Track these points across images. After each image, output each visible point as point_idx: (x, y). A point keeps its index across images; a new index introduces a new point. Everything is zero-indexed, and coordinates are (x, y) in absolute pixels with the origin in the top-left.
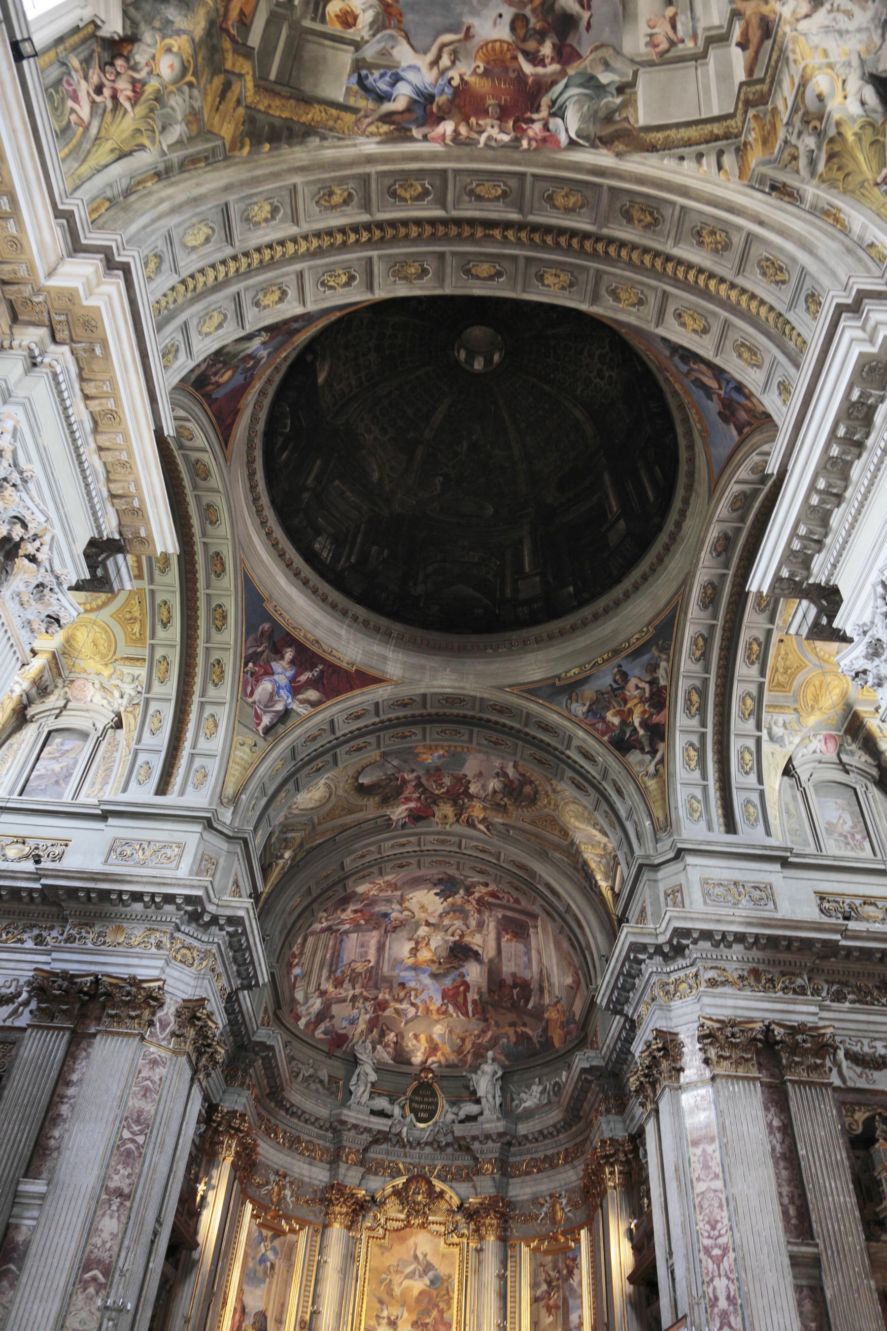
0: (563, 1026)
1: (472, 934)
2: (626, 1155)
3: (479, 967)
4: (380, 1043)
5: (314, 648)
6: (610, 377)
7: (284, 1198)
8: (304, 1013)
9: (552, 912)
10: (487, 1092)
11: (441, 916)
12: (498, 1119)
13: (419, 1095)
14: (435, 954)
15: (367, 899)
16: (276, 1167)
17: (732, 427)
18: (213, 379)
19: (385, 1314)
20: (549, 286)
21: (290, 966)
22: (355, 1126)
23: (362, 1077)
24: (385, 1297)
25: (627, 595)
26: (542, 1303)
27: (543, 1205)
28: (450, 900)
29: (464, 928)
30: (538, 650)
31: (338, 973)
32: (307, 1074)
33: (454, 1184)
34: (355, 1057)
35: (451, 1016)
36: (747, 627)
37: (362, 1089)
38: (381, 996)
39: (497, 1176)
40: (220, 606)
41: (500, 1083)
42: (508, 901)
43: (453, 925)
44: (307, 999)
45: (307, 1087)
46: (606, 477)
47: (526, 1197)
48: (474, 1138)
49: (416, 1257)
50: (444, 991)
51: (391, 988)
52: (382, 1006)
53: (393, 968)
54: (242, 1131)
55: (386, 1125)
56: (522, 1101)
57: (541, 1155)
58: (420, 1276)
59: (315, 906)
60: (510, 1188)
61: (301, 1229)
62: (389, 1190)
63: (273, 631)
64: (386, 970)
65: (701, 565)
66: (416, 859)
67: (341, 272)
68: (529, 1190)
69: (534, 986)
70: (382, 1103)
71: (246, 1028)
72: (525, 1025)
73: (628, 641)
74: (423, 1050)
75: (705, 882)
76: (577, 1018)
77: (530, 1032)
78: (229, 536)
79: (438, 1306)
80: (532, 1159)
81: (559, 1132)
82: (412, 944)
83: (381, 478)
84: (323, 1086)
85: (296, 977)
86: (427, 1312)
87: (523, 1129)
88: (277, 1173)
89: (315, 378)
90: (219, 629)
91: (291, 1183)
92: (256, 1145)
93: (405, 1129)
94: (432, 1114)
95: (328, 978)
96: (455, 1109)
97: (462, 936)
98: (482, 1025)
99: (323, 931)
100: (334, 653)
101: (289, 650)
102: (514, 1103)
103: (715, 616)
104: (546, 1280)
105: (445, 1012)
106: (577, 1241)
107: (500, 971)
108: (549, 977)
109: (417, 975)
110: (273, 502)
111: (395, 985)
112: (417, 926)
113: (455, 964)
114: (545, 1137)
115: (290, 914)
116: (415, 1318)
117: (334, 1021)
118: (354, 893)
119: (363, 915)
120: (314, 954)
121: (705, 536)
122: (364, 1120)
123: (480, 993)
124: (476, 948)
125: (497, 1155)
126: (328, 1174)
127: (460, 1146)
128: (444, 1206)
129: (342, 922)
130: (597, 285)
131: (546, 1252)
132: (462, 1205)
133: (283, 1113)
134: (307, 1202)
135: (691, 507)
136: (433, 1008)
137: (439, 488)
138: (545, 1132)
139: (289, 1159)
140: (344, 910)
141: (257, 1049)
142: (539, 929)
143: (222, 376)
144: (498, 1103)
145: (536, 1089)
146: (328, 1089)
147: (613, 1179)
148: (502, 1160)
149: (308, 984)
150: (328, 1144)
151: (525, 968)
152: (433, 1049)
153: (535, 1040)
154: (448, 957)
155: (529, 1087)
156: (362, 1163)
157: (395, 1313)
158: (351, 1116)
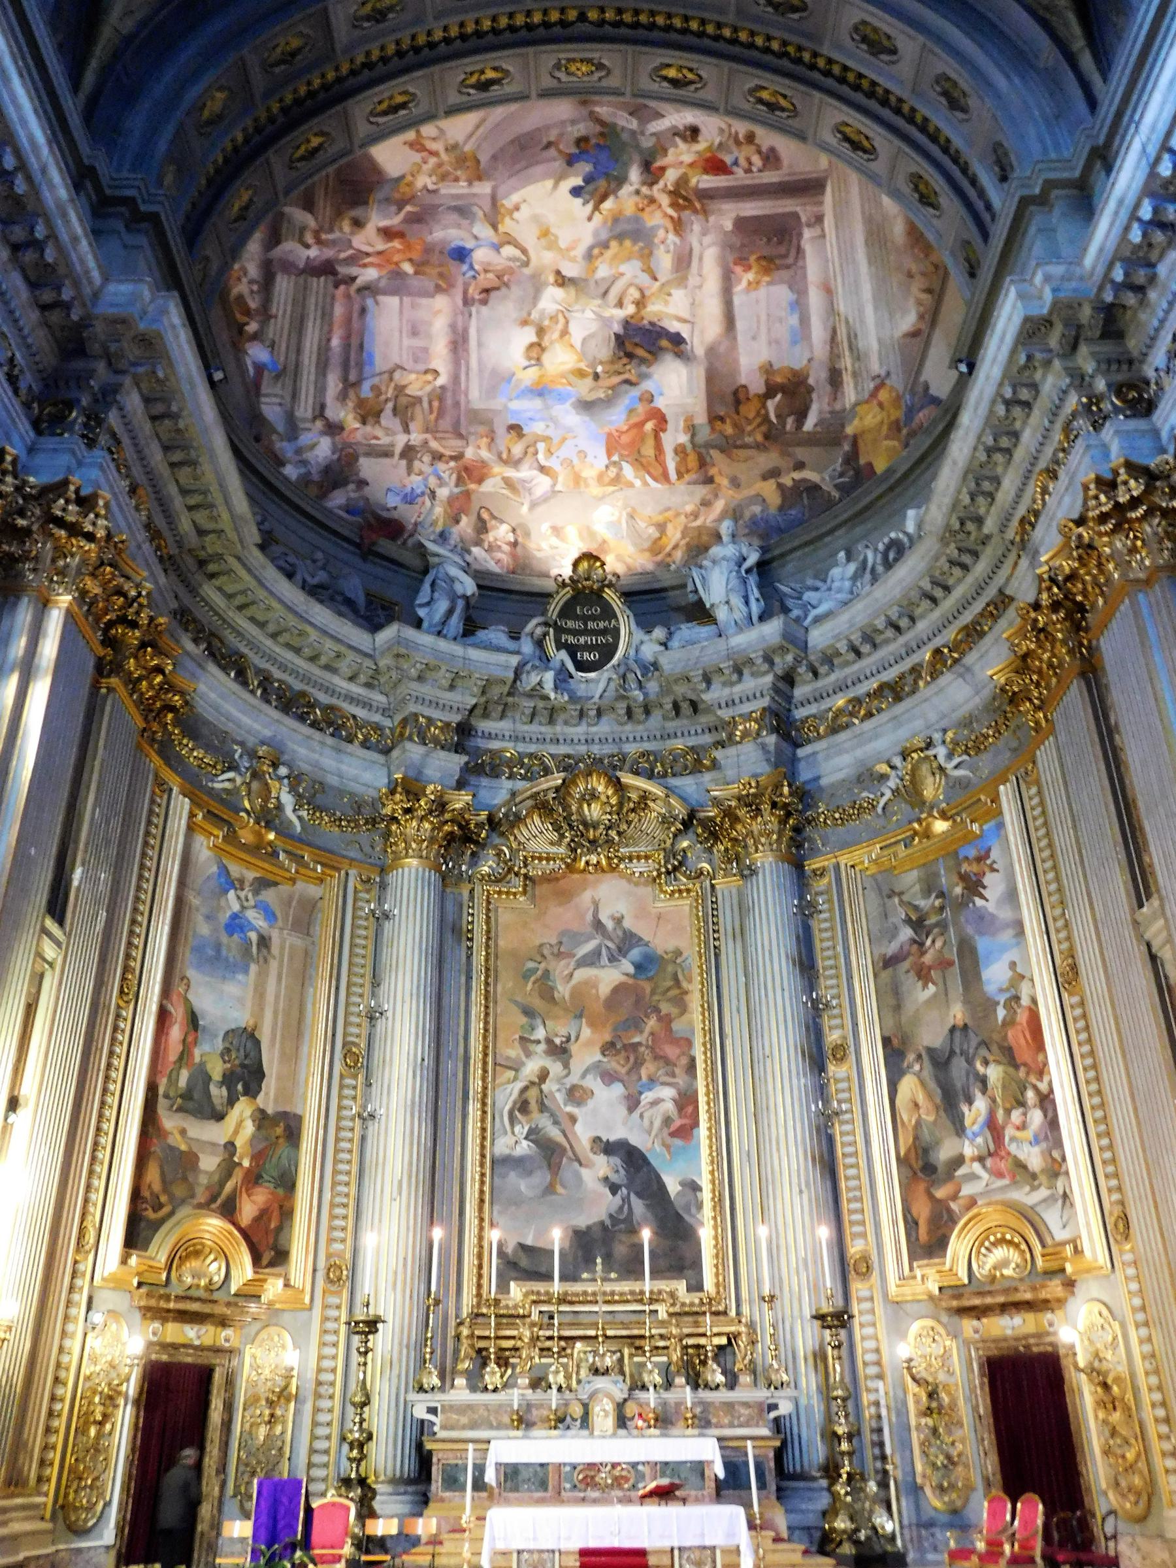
0: (896, 427)
4: (478, 543)
7: (279, 807)
11: (589, 256)
13: (576, 618)
14: (583, 355)
19: (540, 1033)
24: (537, 1003)
26: (906, 965)
27: (883, 777)
28: (608, 205)
29: (644, 280)
31: (366, 390)
33: (674, 782)
38: (469, 453)
41: (753, 580)
42: (748, 171)
43: (614, 279)
47: (840, 776)
49: (598, 925)
50: (609, 435)
56: (807, 607)
58: (612, 959)
60: (802, 766)
64: (475, 395)
69: (817, 377)
72: (800, 466)
79: (657, 1010)
82: (529, 335)
84: (356, 611)
85: (260, 368)
86: (636, 1024)
94: (608, 652)
95: (343, 397)
97: (640, 304)
98: (702, 491)
104: (908, 921)
107: (734, 371)
108: (852, 338)
109: (547, 407)
111: (501, 430)
113: (632, 373)
116: (608, 1037)
119: (409, 247)
120: (299, 325)
123: (692, 429)
124: (674, 326)
125: (765, 702)
127: (676, 707)
129: (357, 258)
132: (692, 815)
136: (589, 473)
140: (358, 224)
142: (829, 222)
144: (755, 609)
145: (842, 572)
149: (295, 395)
150: (377, 718)
151: (794, 343)
154: (615, 359)
157: (563, 1031)
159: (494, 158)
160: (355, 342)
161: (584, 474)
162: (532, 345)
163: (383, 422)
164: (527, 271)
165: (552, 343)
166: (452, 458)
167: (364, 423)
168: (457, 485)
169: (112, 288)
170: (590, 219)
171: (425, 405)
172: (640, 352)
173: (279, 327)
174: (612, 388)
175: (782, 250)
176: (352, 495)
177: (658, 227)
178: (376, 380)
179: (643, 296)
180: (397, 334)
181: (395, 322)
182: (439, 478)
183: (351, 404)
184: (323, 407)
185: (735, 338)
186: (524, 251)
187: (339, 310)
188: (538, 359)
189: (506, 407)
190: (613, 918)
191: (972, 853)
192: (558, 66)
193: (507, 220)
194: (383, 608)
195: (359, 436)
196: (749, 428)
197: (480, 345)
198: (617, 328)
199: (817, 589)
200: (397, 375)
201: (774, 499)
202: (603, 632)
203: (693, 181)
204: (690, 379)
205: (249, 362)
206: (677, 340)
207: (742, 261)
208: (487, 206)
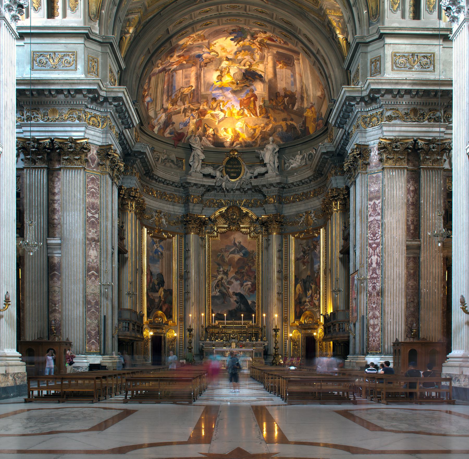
1: (257, 64)
2: (344, 196)
3: (262, 85)
4: (204, 135)
7: (162, 223)
8: (156, 123)
9: (309, 52)
10: (270, 161)
11: (236, 53)
12: (277, 175)
13: (230, 164)
15: (186, 48)
16: (155, 209)
21: (144, 97)
22: (195, 184)
23: (196, 157)
28: (241, 43)
31: (173, 96)
32: (163, 158)
33: (253, 209)
34: (190, 146)
35: (247, 116)
37: (197, 164)
38: (201, 107)
39: (277, 204)
41: (277, 154)
42: (280, 43)
43: (243, 59)
44: (156, 114)
45: (165, 165)
48: (264, 186)
49: (235, 244)
50: (241, 100)
51: (207, 102)
52: (203, 113)
53: (207, 89)
54: (136, 197)
55: (213, 182)
57: (300, 192)
58: (238, 252)
59: (153, 59)
61: (173, 236)
62: (217, 214)
66: (217, 19)
68: (294, 210)
69: (298, 96)
70: (209, 170)
71: (129, 145)
72: (292, 120)
74: (230, 138)
75: (394, 55)
76: (323, 116)
77: (295, 124)
80: (296, 194)
81: (311, 181)
82: (218, 73)
84: (174, 164)
85: (148, 103)
86: (243, 268)
87: (291, 180)
88: (156, 212)
91: (164, 215)
92: (144, 201)
93: (224, 184)
94: (238, 174)
95: (168, 100)
96: (252, 171)
97: (250, 66)
98: (266, 120)
99: (160, 72)
102: (286, 165)
105: (243, 114)
106: (319, 233)
107: (276, 87)
108: (307, 91)
109: (223, 92)
111: (210, 100)
112: (221, 61)
114: (303, 184)
115: (139, 68)
117: (175, 125)
118: (178, 46)
119: (185, 58)
120: (156, 87)
122: (200, 181)
123: (264, 101)
124: (260, 73)
125: (276, 194)
126: (184, 209)
127: (255, 190)
128: (248, 220)
129: (172, 64)
131: (303, 239)
132: (258, 219)
133: (154, 181)
134: (174, 223)
136: (235, 111)
138: (303, 181)
139: (161, 204)
140: (172, 57)
141: (136, 154)
142: (301, 61)
144: (276, 166)
145: (299, 157)
146: (177, 165)
147: (336, 207)
148: (279, 196)
149: (156, 106)
152: (237, 136)
153: (298, 129)
154: (243, 79)
155: (294, 156)
156: (201, 202)
158: (192, 179)
159: (209, 35)
160: (170, 85)
161: (234, 112)
162: (219, 76)
163: (178, 104)
164: (217, 57)
165: (225, 75)
166: (197, 110)
167: (173, 106)
168: (198, 118)
169: (136, 145)
170: (236, 45)
171: (189, 96)
172: (250, 78)
173: (152, 91)
174: (242, 87)
175: (290, 62)
176: (171, 128)
177: (255, 49)
178: (176, 93)
179: (251, 64)
180: (181, 79)
181: (181, 76)
182: (193, 116)
183: (169, 102)
184: (163, 105)
185: (277, 79)
186: (217, 53)
187: (166, 78)
188: (221, 79)
189: (211, 93)
190: (238, 242)
191: (316, 240)
192: (228, 20)
193: (212, 47)
194: (181, 161)
195: (172, 110)
196: (280, 104)
197: (204, 77)
198: (243, 71)
199: (293, 159)
200: (181, 90)
201: (285, 128)
202: (238, 168)
203: (265, 41)
204: (264, 87)
205: (146, 103)
206: (260, 76)
207: (278, 61)
208: (207, 45)
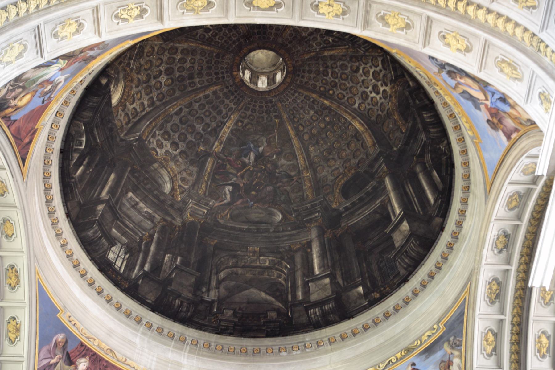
5: (108, 358)
6: (384, 91)
17: (501, 133)
18: (13, 103)
20: (323, 14)
25: (415, 294)
30: (332, 351)
36: (534, 321)
40: (14, 318)
46: (388, 182)
63: (66, 342)
65: (484, 262)
67: (133, 6)
73: (420, 338)
78: (24, 249)
83: (173, 189)
89: (110, 99)
90: (12, 342)
100: (129, 362)
101: (83, 360)
103: (502, 311)
110: (68, 215)
121: (486, 234)
130: (367, 12)
135: (470, 207)
137: (228, 197)
143: (21, 100)
